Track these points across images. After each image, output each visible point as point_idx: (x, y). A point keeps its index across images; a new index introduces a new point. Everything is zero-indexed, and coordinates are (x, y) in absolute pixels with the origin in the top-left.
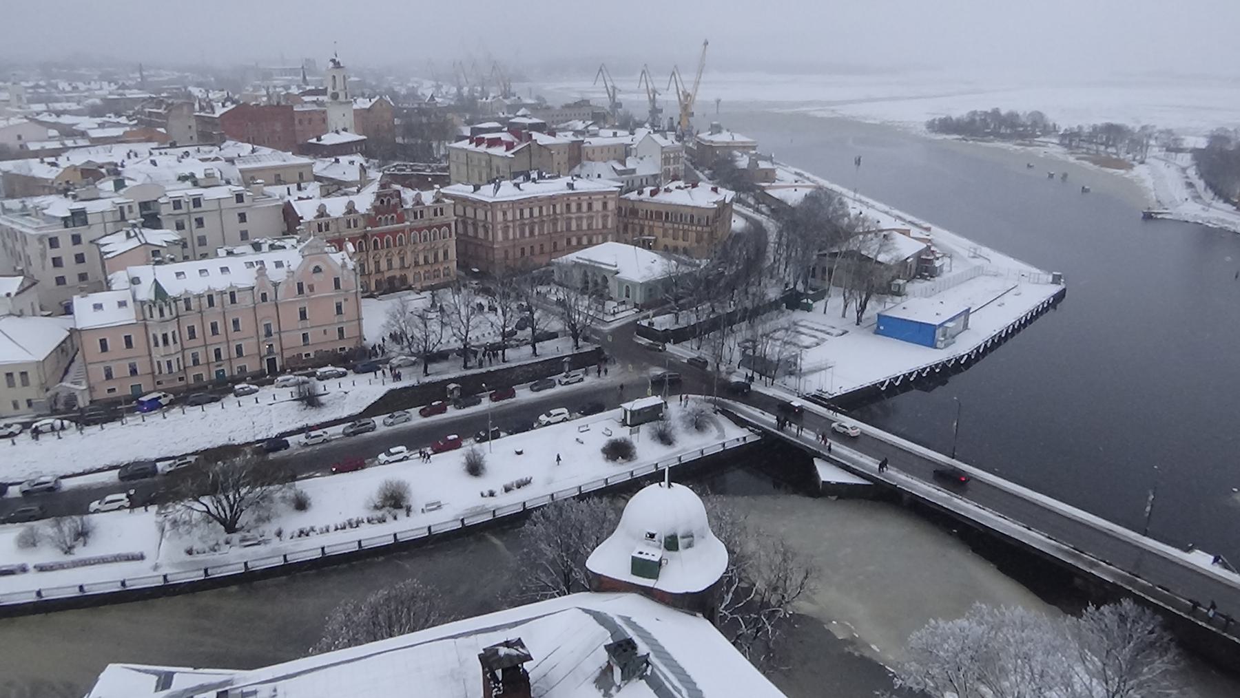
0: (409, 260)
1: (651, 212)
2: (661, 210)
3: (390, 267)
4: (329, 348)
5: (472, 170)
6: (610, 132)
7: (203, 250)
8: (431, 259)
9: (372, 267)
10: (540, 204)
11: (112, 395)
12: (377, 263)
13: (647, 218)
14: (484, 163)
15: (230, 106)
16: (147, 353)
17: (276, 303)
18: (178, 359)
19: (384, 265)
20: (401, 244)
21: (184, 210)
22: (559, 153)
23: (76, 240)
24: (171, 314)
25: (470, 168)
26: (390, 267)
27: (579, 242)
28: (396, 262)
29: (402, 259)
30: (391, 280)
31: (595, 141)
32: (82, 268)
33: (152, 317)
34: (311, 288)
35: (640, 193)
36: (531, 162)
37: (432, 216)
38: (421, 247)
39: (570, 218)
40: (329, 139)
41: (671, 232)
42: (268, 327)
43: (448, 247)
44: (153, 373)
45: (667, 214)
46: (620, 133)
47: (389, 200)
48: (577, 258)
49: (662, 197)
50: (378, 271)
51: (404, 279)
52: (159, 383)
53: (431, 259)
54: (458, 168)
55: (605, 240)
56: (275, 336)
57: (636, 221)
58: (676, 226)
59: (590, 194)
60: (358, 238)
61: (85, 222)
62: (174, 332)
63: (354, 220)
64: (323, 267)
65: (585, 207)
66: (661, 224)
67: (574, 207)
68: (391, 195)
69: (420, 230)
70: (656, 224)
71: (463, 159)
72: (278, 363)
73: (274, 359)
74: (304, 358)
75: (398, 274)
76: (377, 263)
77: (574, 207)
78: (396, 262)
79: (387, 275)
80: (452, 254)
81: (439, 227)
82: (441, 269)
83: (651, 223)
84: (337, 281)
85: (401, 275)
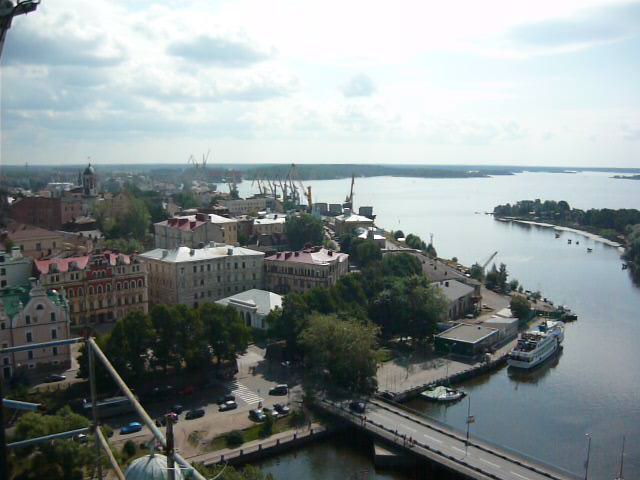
0: (115, 300)
3: (101, 307)
4: (46, 361)
6: (273, 215)
8: (130, 301)
9: (88, 306)
12: (92, 304)
15: (19, 199)
19: (96, 305)
20: (109, 290)
26: (101, 307)
28: (105, 304)
29: (109, 301)
30: (101, 315)
31: (263, 222)
34: (35, 320)
35: (279, 256)
37: (131, 272)
38: (122, 293)
40: (79, 220)
41: (299, 282)
46: (279, 215)
49: (293, 259)
50: (92, 309)
51: (110, 315)
53: (130, 301)
55: (254, 288)
57: (276, 275)
58: (302, 277)
59: (244, 257)
64: (43, 305)
65: (240, 265)
69: (122, 281)
72: (11, 371)
73: (8, 369)
75: (105, 311)
76: (92, 304)
77: (232, 265)
78: (105, 304)
79: (98, 312)
80: (146, 297)
81: (136, 279)
84: (53, 315)
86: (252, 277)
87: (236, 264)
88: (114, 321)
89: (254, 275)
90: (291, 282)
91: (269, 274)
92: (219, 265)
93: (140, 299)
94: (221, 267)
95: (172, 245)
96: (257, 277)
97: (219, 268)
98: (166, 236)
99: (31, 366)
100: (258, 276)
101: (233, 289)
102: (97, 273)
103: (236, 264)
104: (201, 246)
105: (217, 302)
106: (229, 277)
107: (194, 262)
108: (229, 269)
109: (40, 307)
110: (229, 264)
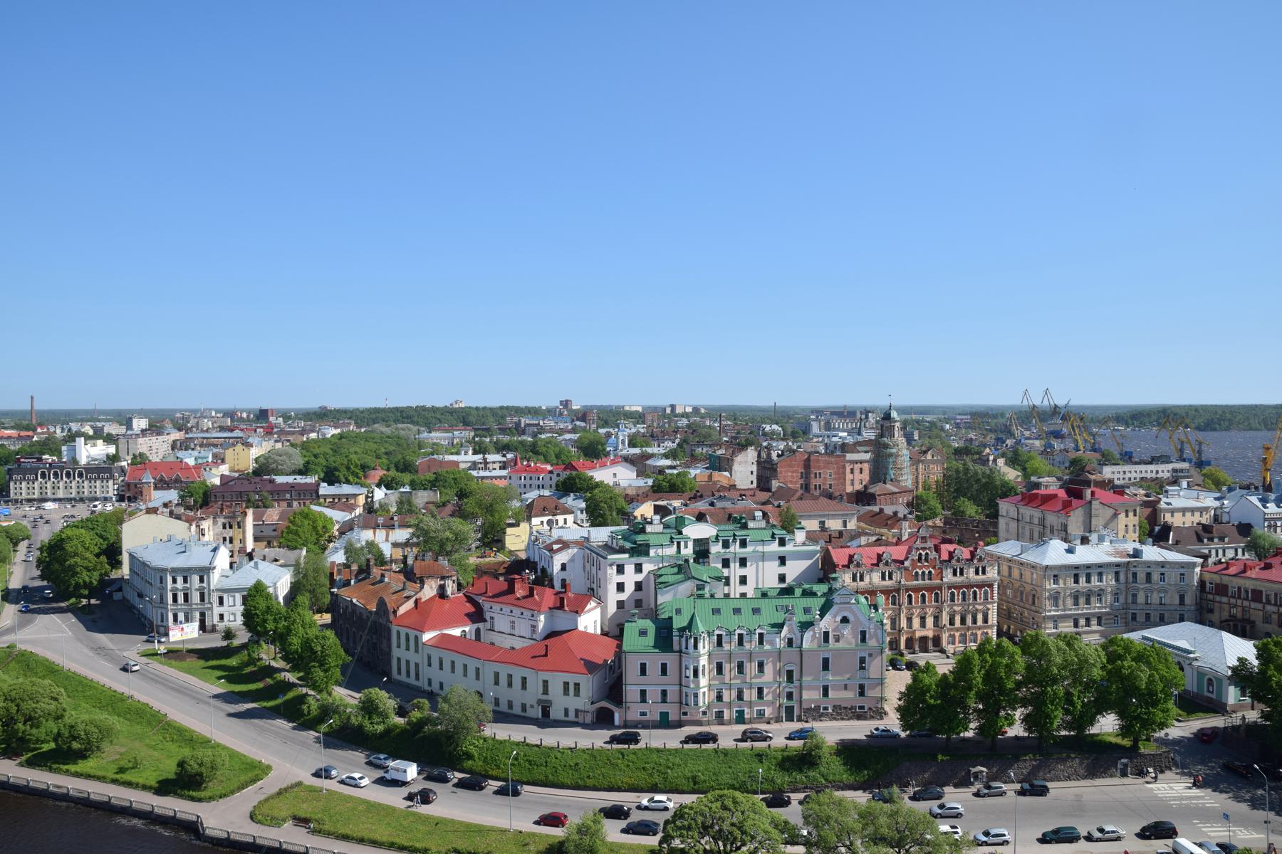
0: (945, 619)
1: (1247, 592)
2: (1258, 588)
5: (1023, 528)
7: (743, 589)
9: (904, 623)
10: (1100, 570)
11: (643, 718)
13: (1239, 597)
14: (1036, 521)
16: (678, 683)
17: (801, 651)
18: (704, 692)
19: (916, 622)
21: (732, 549)
22: (1127, 516)
23: (639, 568)
24: (704, 647)
25: (1020, 525)
27: (1148, 616)
29: (937, 618)
30: (924, 640)
31: (1177, 503)
32: (639, 595)
33: (687, 648)
36: (1090, 522)
39: (1138, 590)
42: (790, 673)
43: (988, 609)
44: (681, 703)
45: (1268, 596)
47: (927, 554)
48: (1144, 638)
51: (937, 641)
52: (685, 714)
54: (1007, 524)
55: (1182, 619)
56: (796, 683)
57: (1225, 599)
59: (1162, 564)
60: (891, 591)
61: (647, 554)
62: (704, 666)
63: (889, 573)
64: (851, 618)
65: (1155, 577)
66: (1259, 606)
67: (1141, 576)
68: (929, 548)
69: (958, 587)
70: (1253, 605)
71: (1013, 513)
74: (821, 711)
75: (930, 634)
77: (1141, 576)
78: (930, 621)
79: (918, 635)
80: (993, 618)
81: (980, 586)
82: (979, 633)
83: (1246, 603)
85: (934, 636)
86: (1177, 601)
87: (1149, 575)
88: (943, 651)
89: (1182, 598)
90: (1257, 616)
91: (1210, 597)
92: (1117, 573)
93: (985, 620)
94: (1122, 577)
95: (1040, 537)
96: (1188, 600)
97: (1117, 580)
98: (1018, 520)
99: (826, 708)
100: (1189, 600)
101: (1141, 618)
102: (920, 572)
103: (1149, 575)
104: (1085, 540)
105: (1125, 636)
106: (1135, 596)
107: (1077, 567)
108: (1135, 580)
109: (845, 620)
110: (1135, 575)
